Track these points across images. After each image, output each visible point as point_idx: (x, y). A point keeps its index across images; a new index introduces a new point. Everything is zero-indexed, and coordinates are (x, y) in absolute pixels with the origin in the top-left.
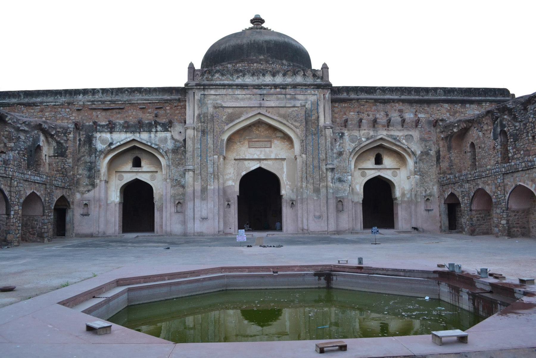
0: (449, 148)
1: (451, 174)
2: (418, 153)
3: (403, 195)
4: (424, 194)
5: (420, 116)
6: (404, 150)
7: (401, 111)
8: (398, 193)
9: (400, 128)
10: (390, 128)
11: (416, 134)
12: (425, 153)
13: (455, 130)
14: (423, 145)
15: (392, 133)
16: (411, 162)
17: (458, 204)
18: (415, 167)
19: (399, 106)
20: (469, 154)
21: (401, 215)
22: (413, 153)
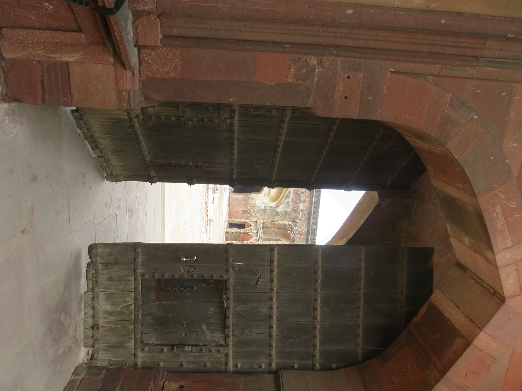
0: (278, 228)
1: (263, 228)
2: (277, 210)
3: (253, 199)
4: (252, 210)
5: (301, 213)
6: (280, 201)
7: (304, 201)
8: (254, 195)
9: (294, 200)
10: (294, 194)
11: (289, 209)
12: (277, 214)
13: (289, 232)
14: (282, 213)
15: (291, 195)
16: (273, 205)
17: (244, 228)
18: (269, 207)
19: (307, 200)
20: (274, 238)
21: (241, 196)
22: (278, 206)
